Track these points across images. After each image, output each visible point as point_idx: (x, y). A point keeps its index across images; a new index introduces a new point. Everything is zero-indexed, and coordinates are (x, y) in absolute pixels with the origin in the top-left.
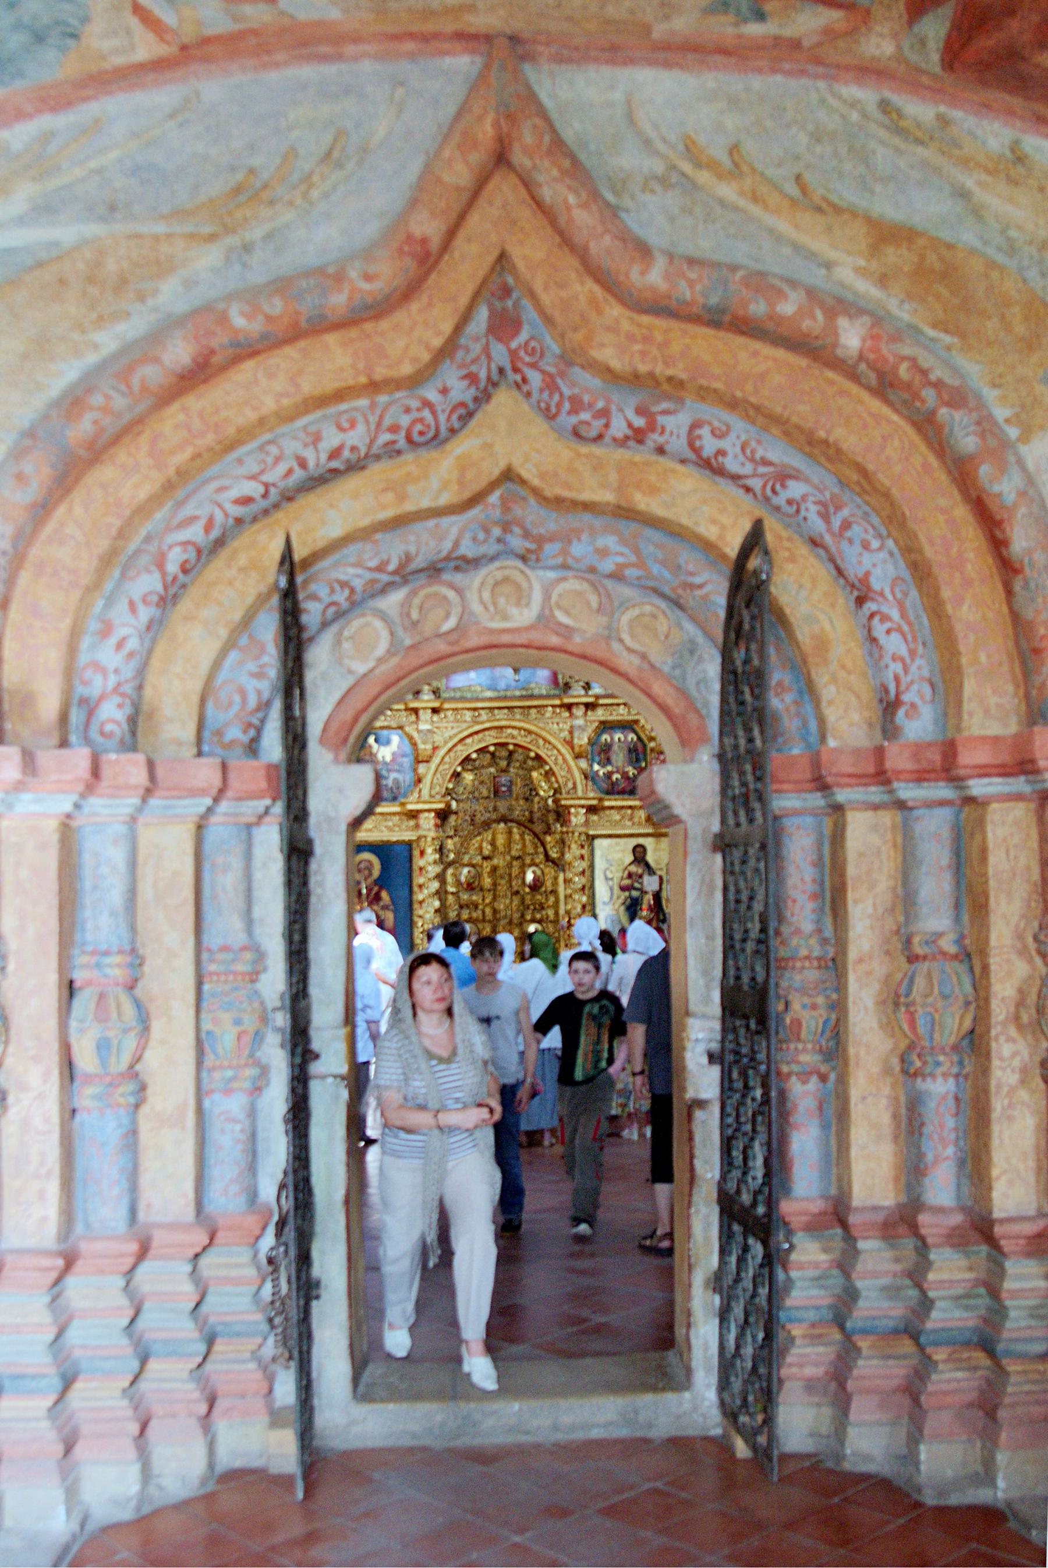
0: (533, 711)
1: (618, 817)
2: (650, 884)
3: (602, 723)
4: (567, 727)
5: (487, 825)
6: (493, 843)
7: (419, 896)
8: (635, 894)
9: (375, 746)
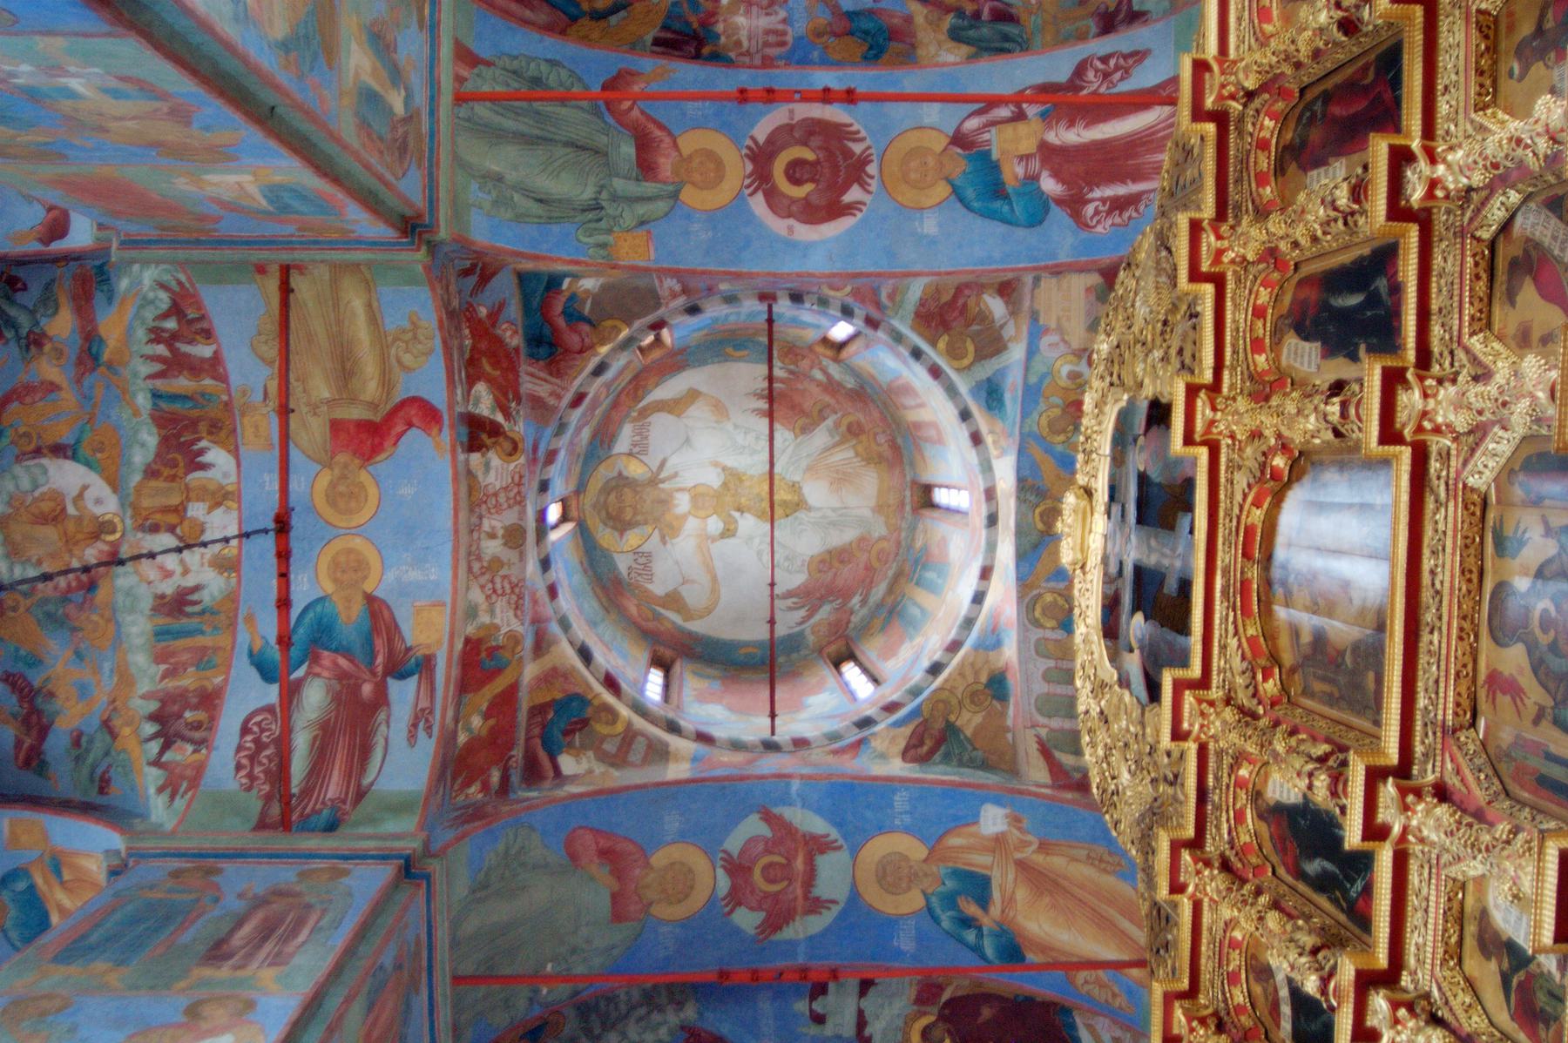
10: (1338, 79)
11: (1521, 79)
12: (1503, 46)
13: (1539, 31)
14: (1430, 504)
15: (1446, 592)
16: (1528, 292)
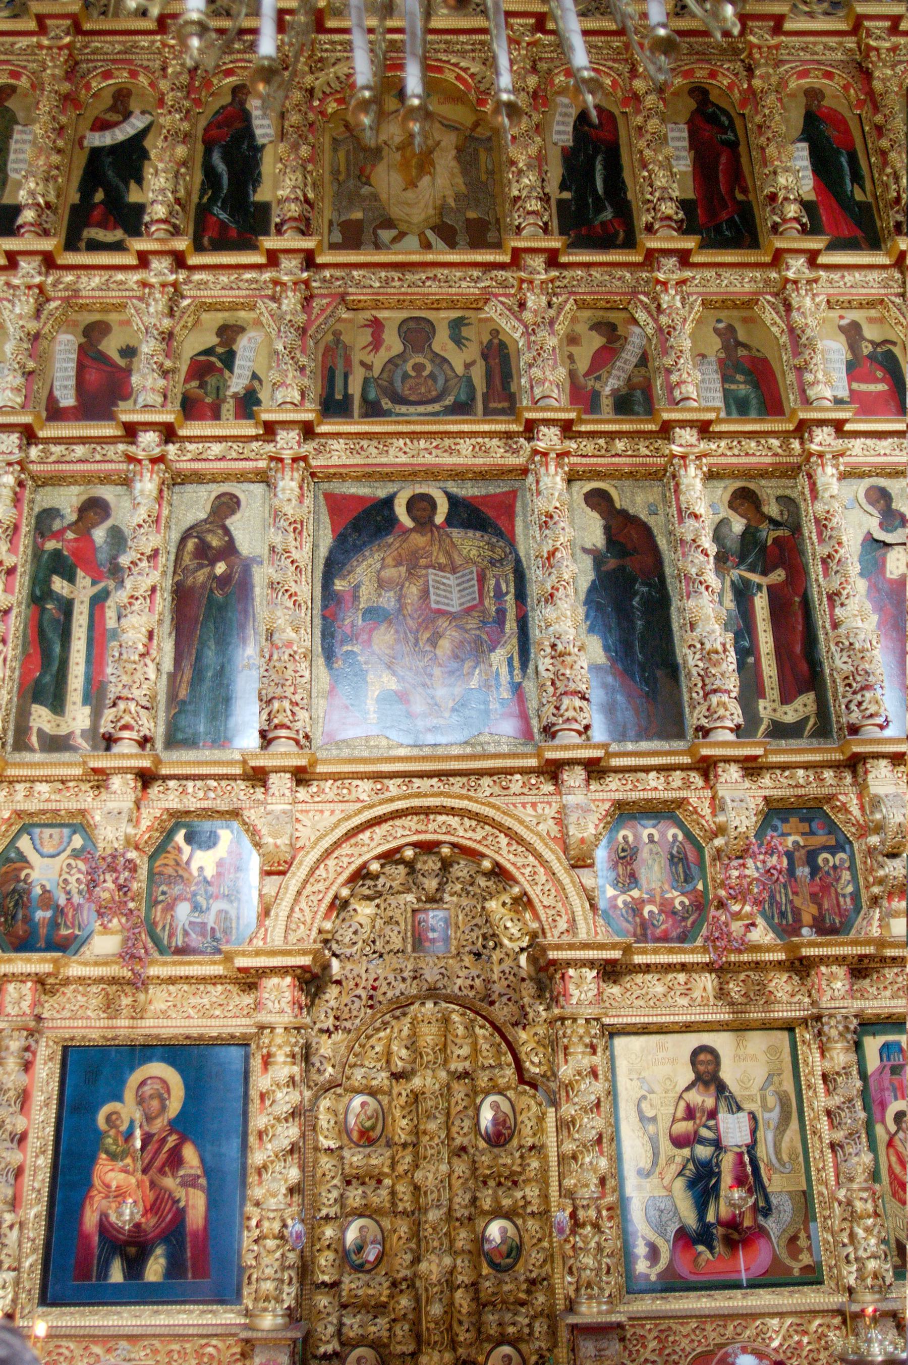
0: (486, 781)
1: (660, 989)
2: (734, 1130)
4: (550, 811)
5: (401, 1006)
6: (412, 1045)
7: (257, 1157)
8: (704, 1152)
9: (187, 849)
10: (744, 160)
11: (716, 330)
12: (735, 313)
13: (739, 344)
14: (476, 273)
15: (426, 290)
16: (598, 341)
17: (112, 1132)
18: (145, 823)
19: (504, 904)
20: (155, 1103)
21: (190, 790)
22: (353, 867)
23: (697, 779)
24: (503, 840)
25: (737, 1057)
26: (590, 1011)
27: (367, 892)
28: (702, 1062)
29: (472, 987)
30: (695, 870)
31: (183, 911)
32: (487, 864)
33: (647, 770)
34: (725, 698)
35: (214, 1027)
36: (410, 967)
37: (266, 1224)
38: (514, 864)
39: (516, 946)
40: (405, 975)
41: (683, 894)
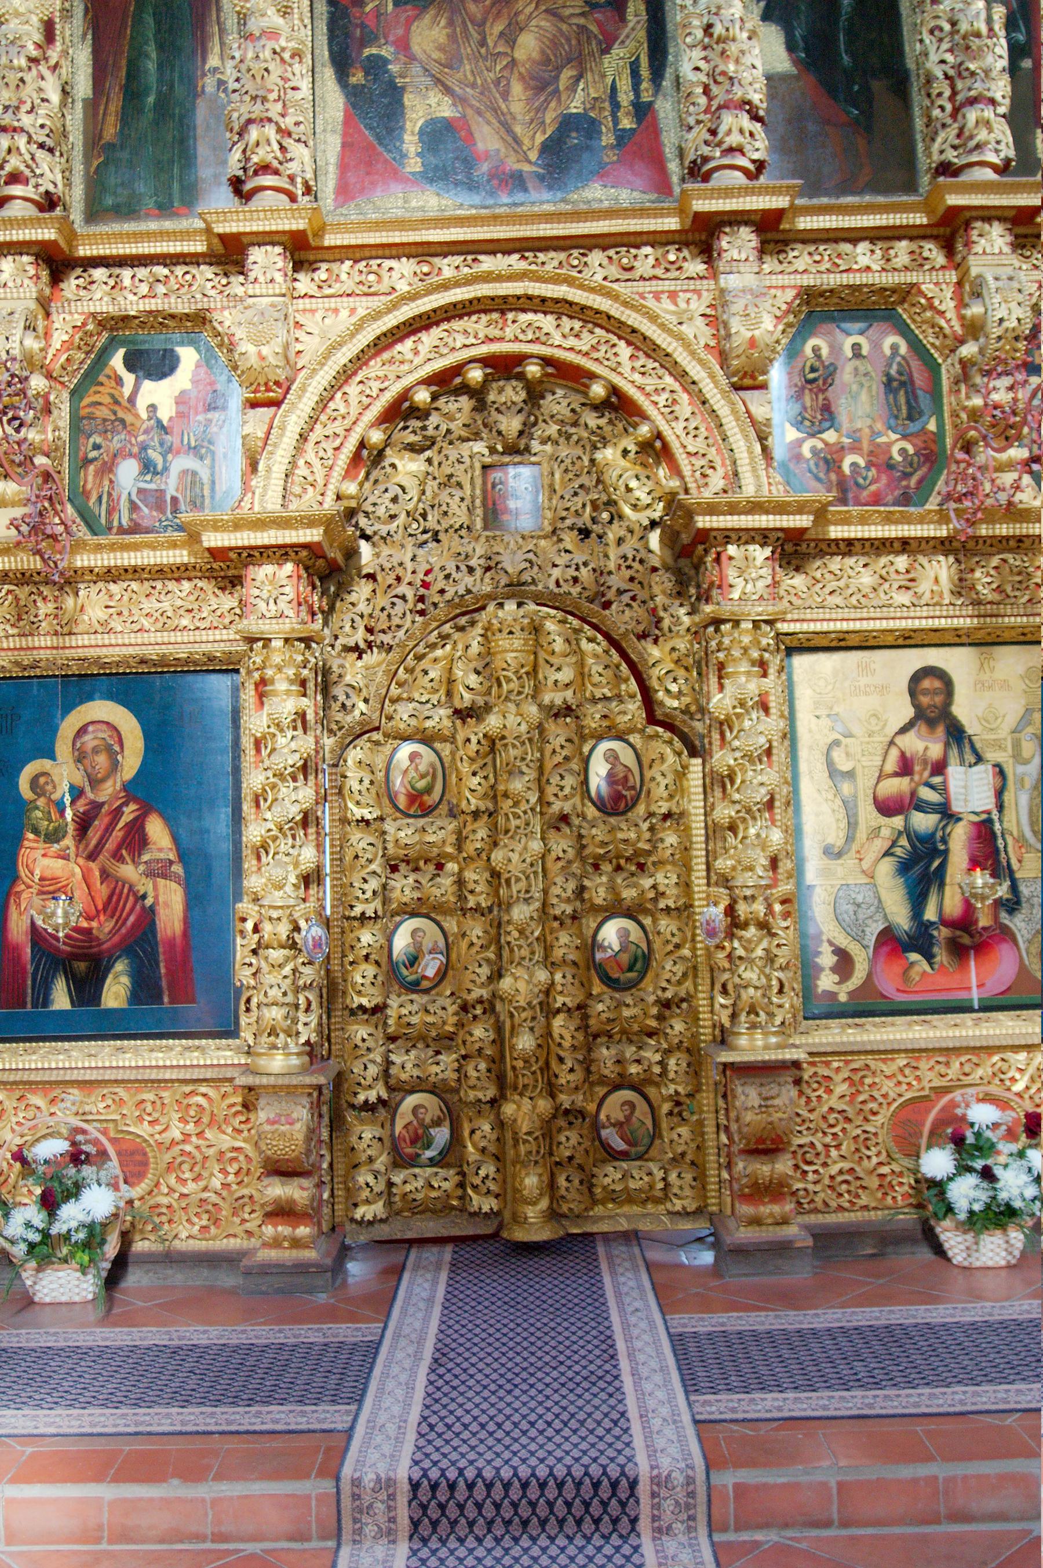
0: (596, 257)
1: (867, 579)
2: (970, 789)
3: (809, 296)
4: (699, 306)
5: (468, 609)
6: (485, 667)
7: (253, 832)
8: (923, 822)
9: (129, 379)
17: (41, 802)
18: (58, 338)
19: (625, 452)
20: (102, 760)
21: (127, 282)
22: (388, 397)
23: (933, 252)
24: (624, 351)
25: (980, 686)
26: (761, 610)
27: (412, 438)
28: (925, 692)
29: (575, 580)
30: (924, 401)
31: (127, 472)
32: (598, 390)
33: (853, 236)
34: (988, 113)
35: (181, 644)
36: (480, 551)
37: (267, 928)
38: (641, 388)
39: (644, 518)
40: (473, 563)
41: (905, 437)
